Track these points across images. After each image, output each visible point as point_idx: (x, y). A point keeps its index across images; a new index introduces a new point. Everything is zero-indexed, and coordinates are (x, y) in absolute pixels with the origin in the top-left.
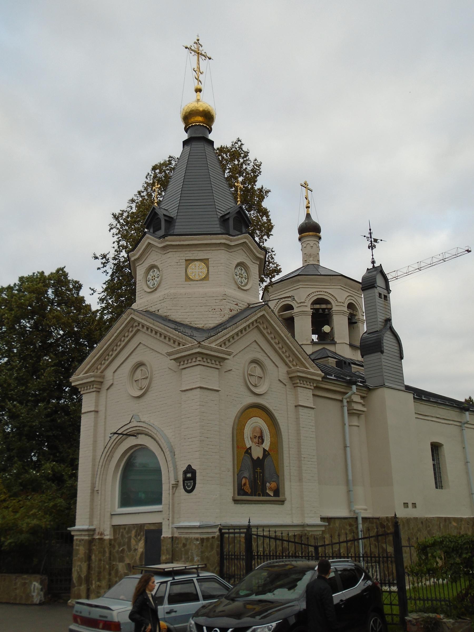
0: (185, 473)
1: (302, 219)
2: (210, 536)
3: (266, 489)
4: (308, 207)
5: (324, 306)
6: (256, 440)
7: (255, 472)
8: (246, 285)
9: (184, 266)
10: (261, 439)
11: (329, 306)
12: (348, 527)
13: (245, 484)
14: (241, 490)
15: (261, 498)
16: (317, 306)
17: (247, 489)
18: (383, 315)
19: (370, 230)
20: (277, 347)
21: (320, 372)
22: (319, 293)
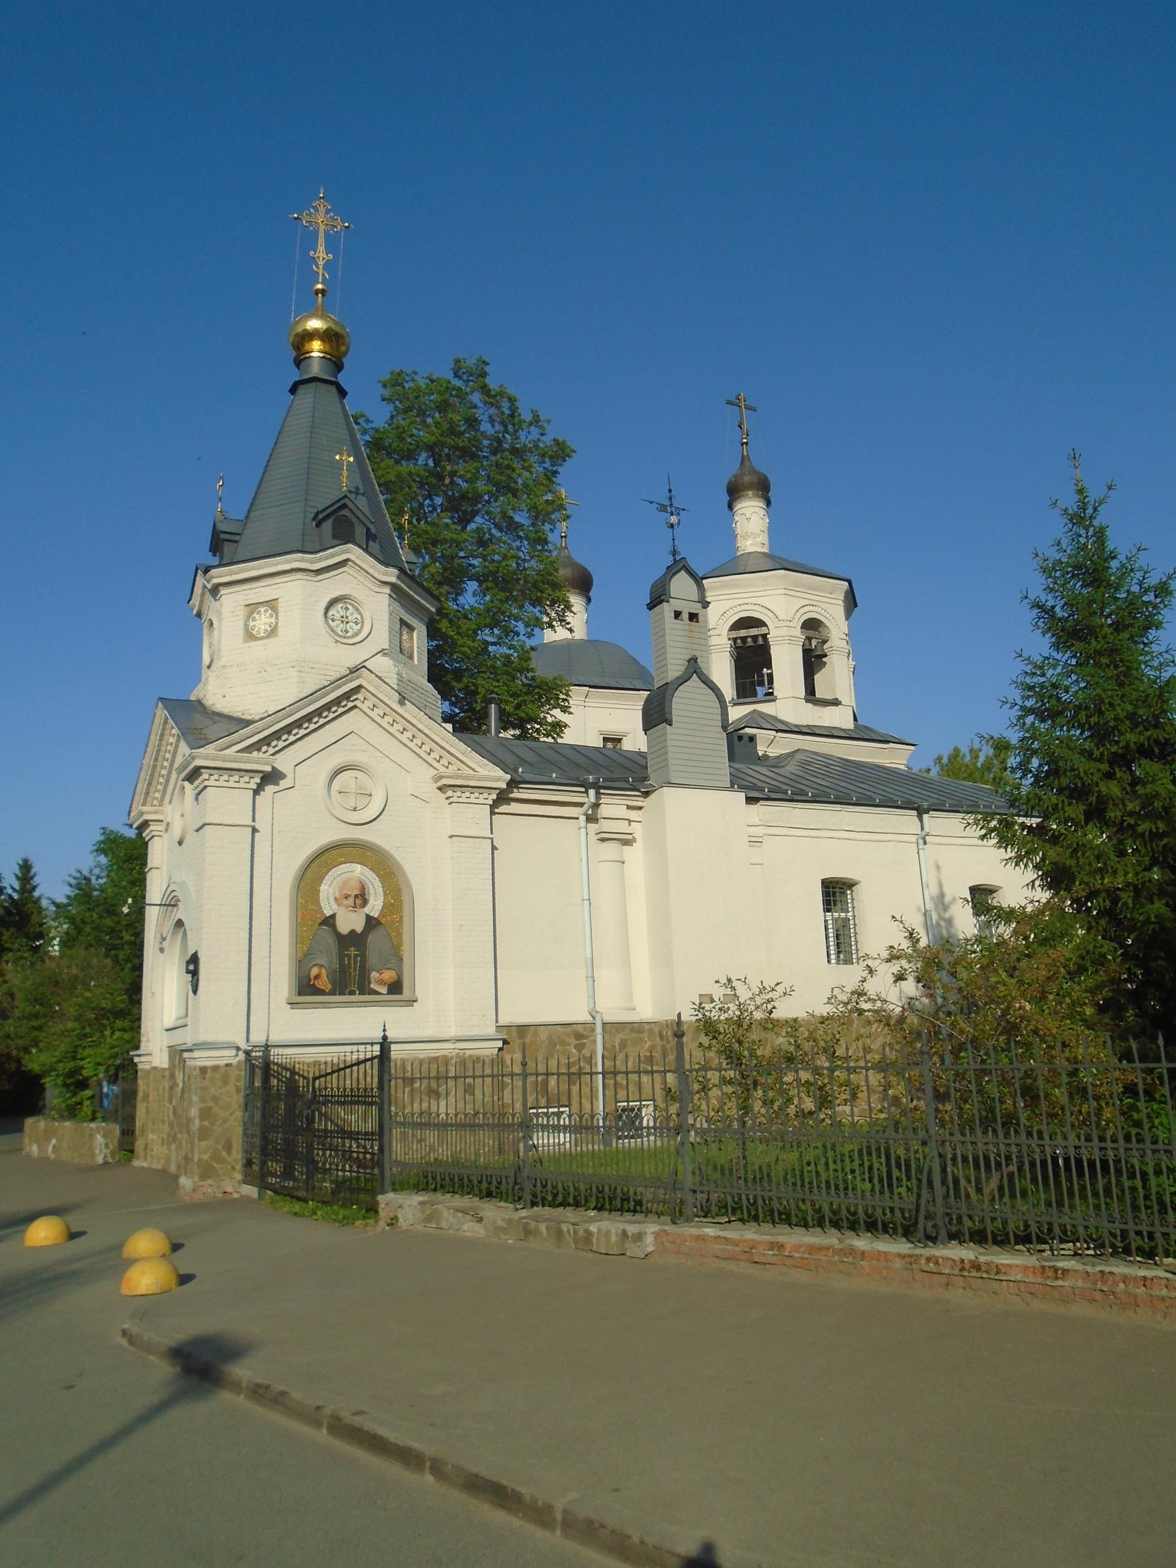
0: (188, 963)
1: (731, 469)
2: (222, 1063)
3: (370, 983)
5: (754, 632)
6: (350, 901)
7: (341, 957)
8: (357, 634)
9: (242, 617)
10: (362, 898)
11: (763, 630)
12: (573, 1041)
13: (317, 977)
14: (305, 988)
15: (357, 997)
16: (743, 633)
17: (324, 983)
18: (683, 651)
19: (670, 491)
20: (404, 738)
21: (499, 772)
22: (739, 608)
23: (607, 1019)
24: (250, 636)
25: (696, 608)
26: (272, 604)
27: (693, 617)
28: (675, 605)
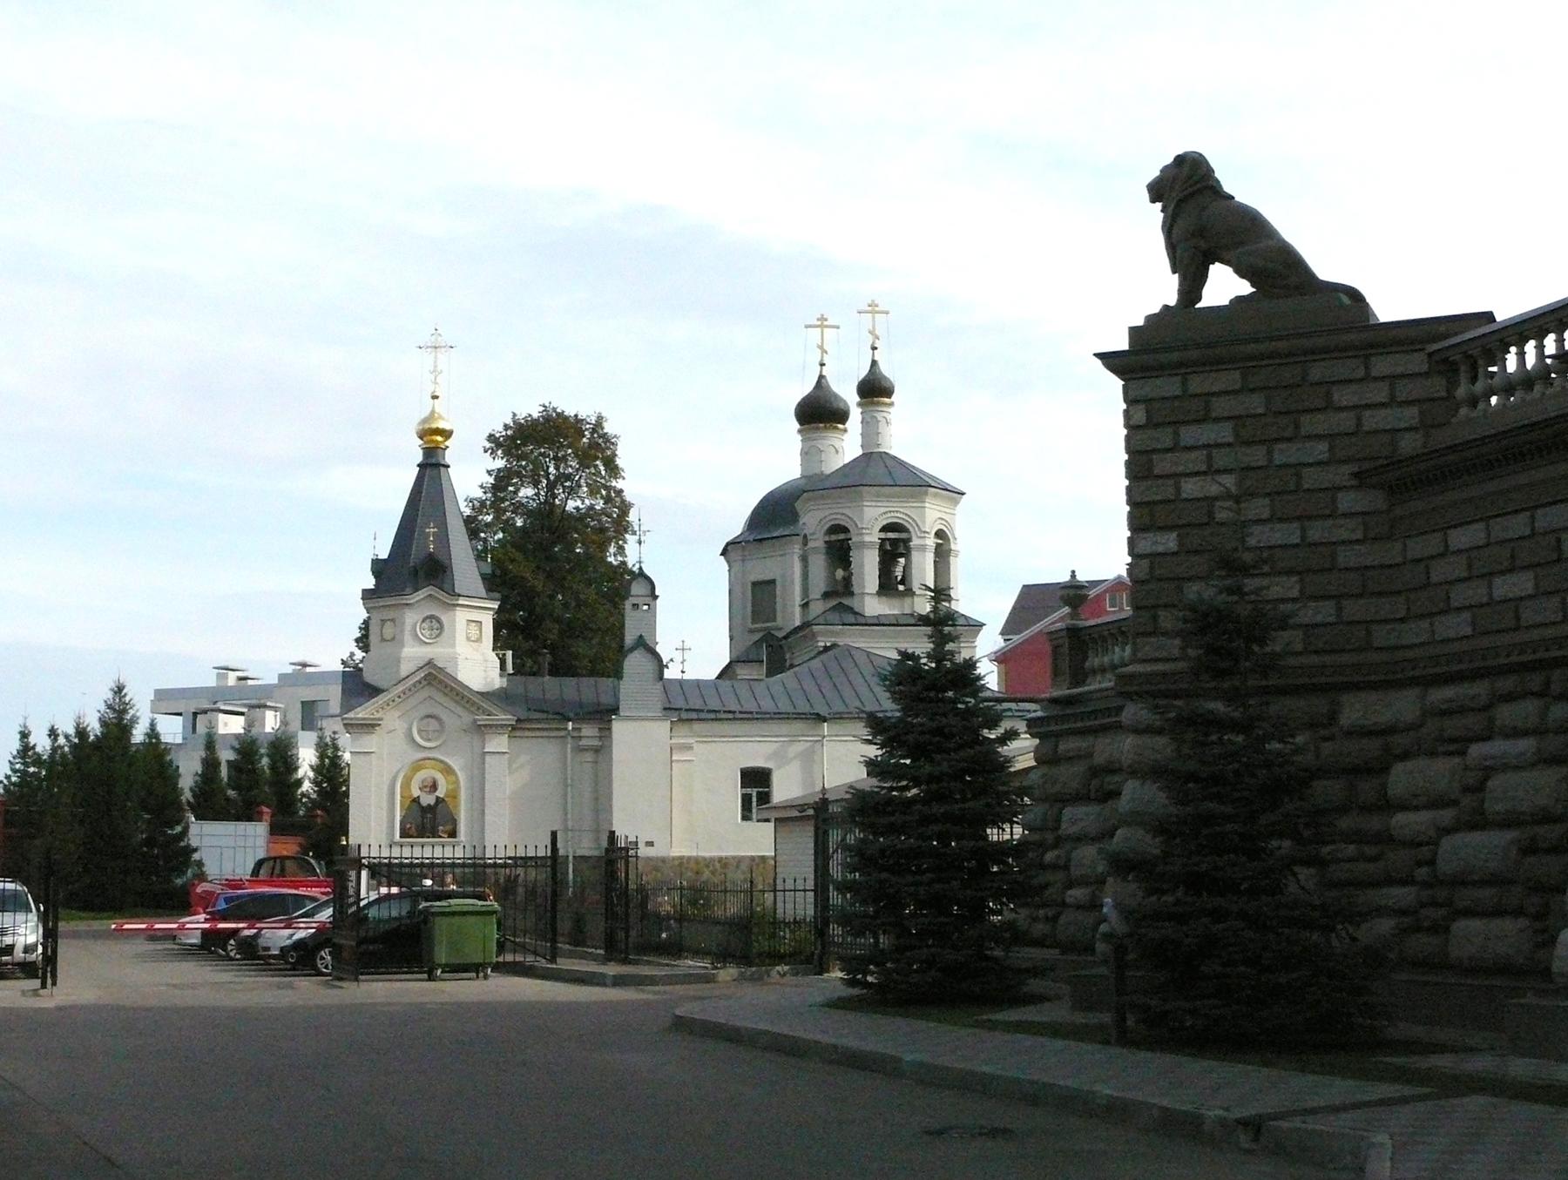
4: (874, 348)
5: (842, 536)
10: (434, 787)
16: (834, 537)
23: (580, 853)
24: (383, 640)
26: (393, 620)
28: (632, 600)
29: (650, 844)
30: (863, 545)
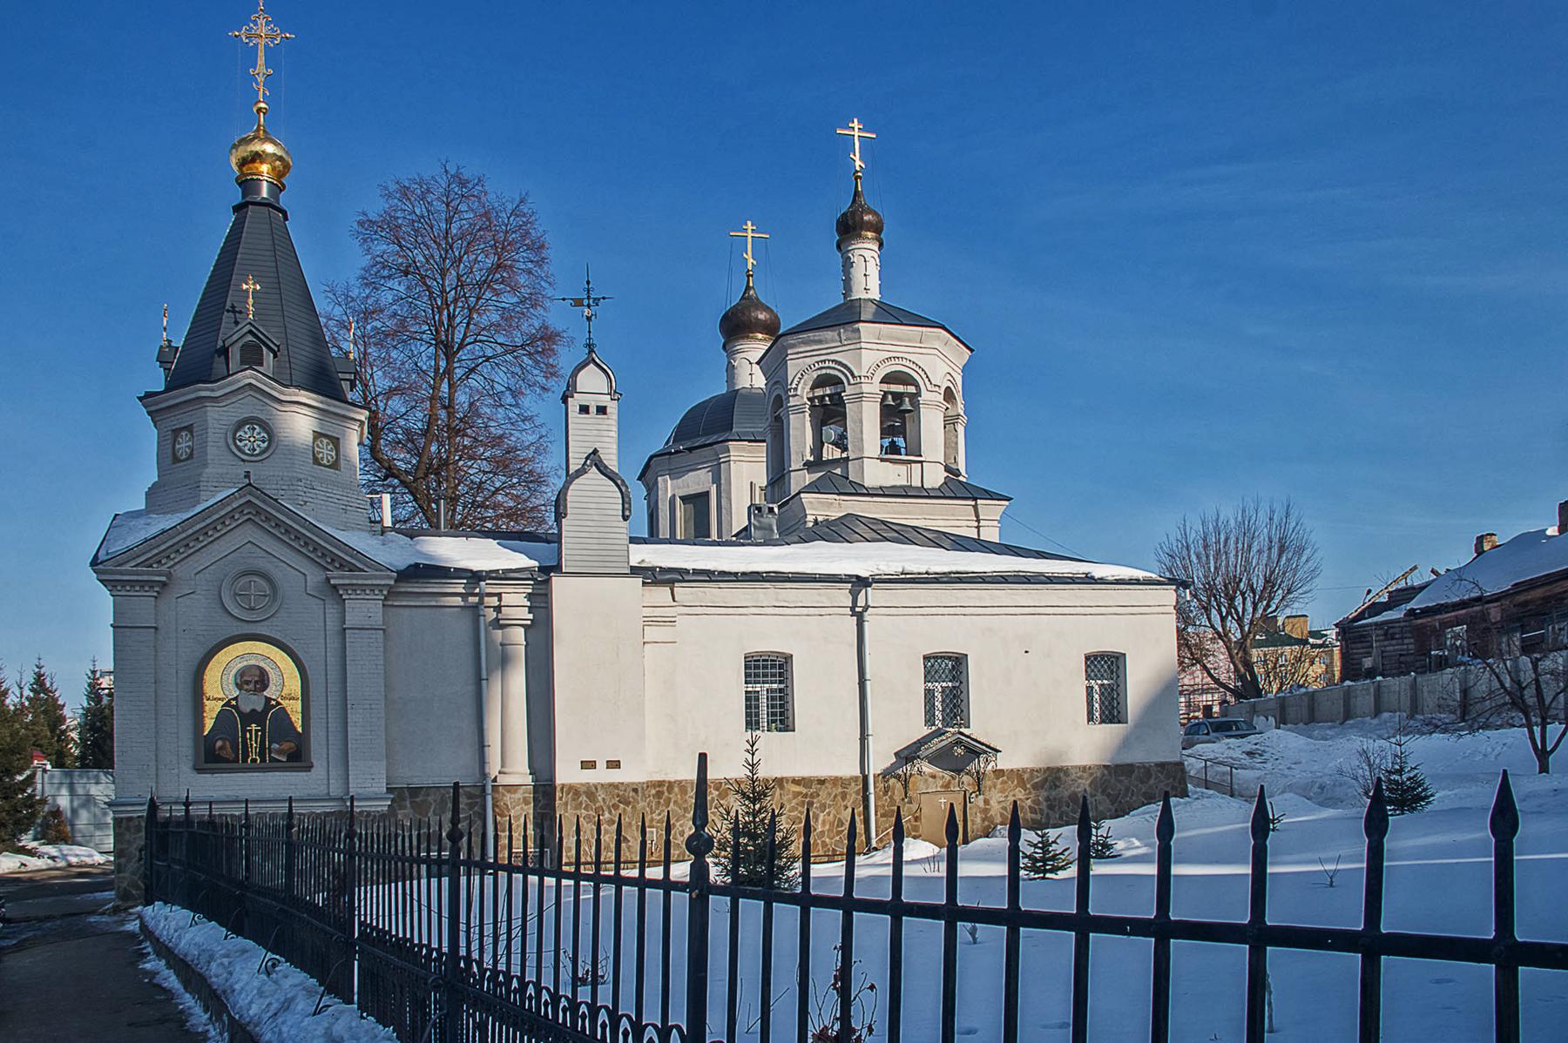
6: (251, 686)
16: (819, 392)
25: (605, 400)
26: (189, 428)
27: (602, 410)
29: (614, 764)
30: (860, 397)
